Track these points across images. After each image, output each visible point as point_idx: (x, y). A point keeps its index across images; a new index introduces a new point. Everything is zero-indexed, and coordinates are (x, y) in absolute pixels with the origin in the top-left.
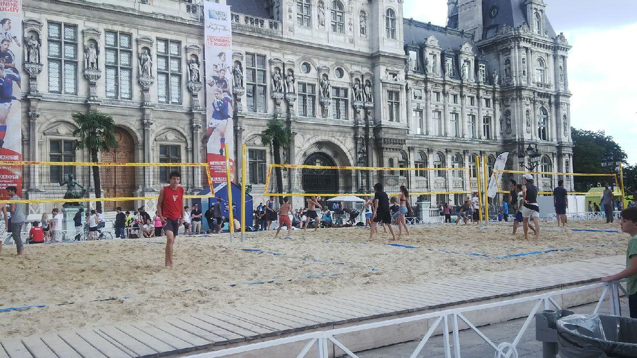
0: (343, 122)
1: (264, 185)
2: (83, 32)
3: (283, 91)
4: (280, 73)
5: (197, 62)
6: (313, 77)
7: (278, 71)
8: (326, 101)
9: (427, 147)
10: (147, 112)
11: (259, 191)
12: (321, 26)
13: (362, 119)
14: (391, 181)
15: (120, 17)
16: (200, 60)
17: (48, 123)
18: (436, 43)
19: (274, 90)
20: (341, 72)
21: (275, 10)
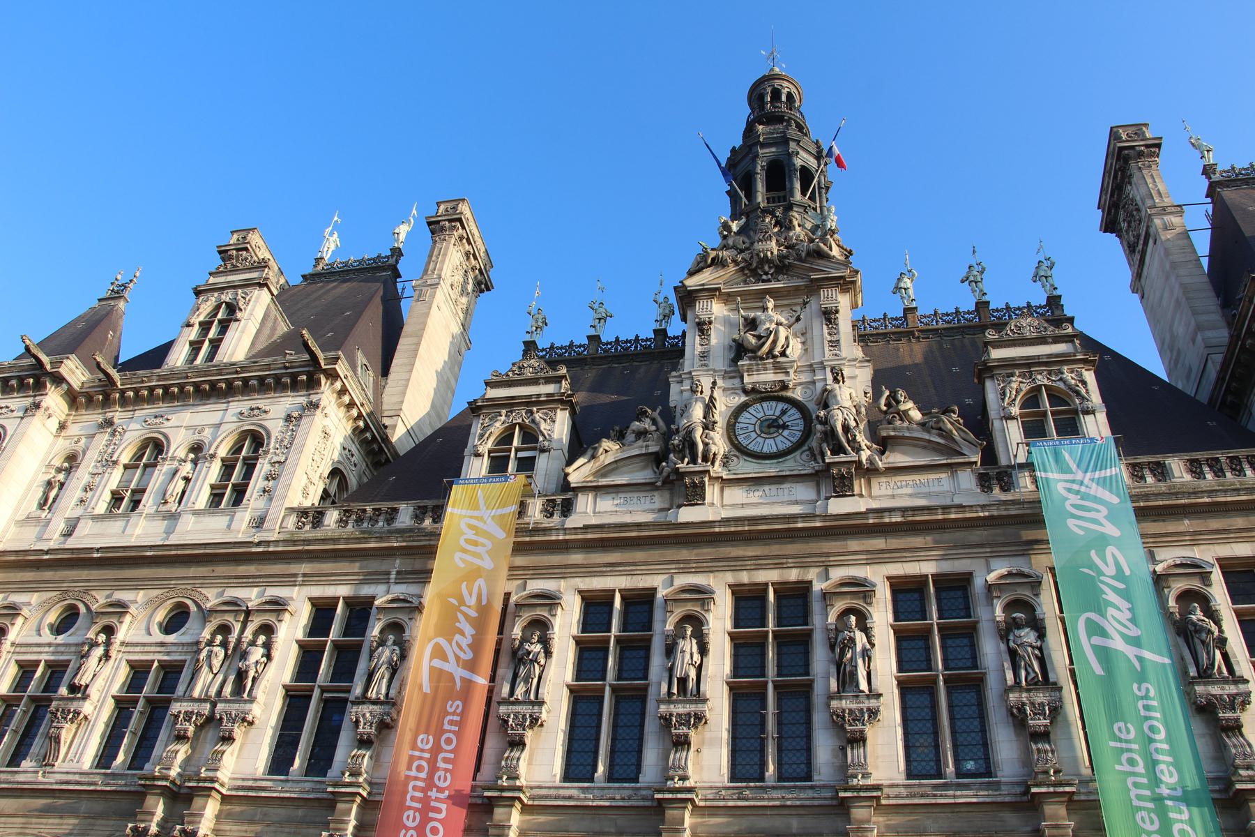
15: (775, 549)
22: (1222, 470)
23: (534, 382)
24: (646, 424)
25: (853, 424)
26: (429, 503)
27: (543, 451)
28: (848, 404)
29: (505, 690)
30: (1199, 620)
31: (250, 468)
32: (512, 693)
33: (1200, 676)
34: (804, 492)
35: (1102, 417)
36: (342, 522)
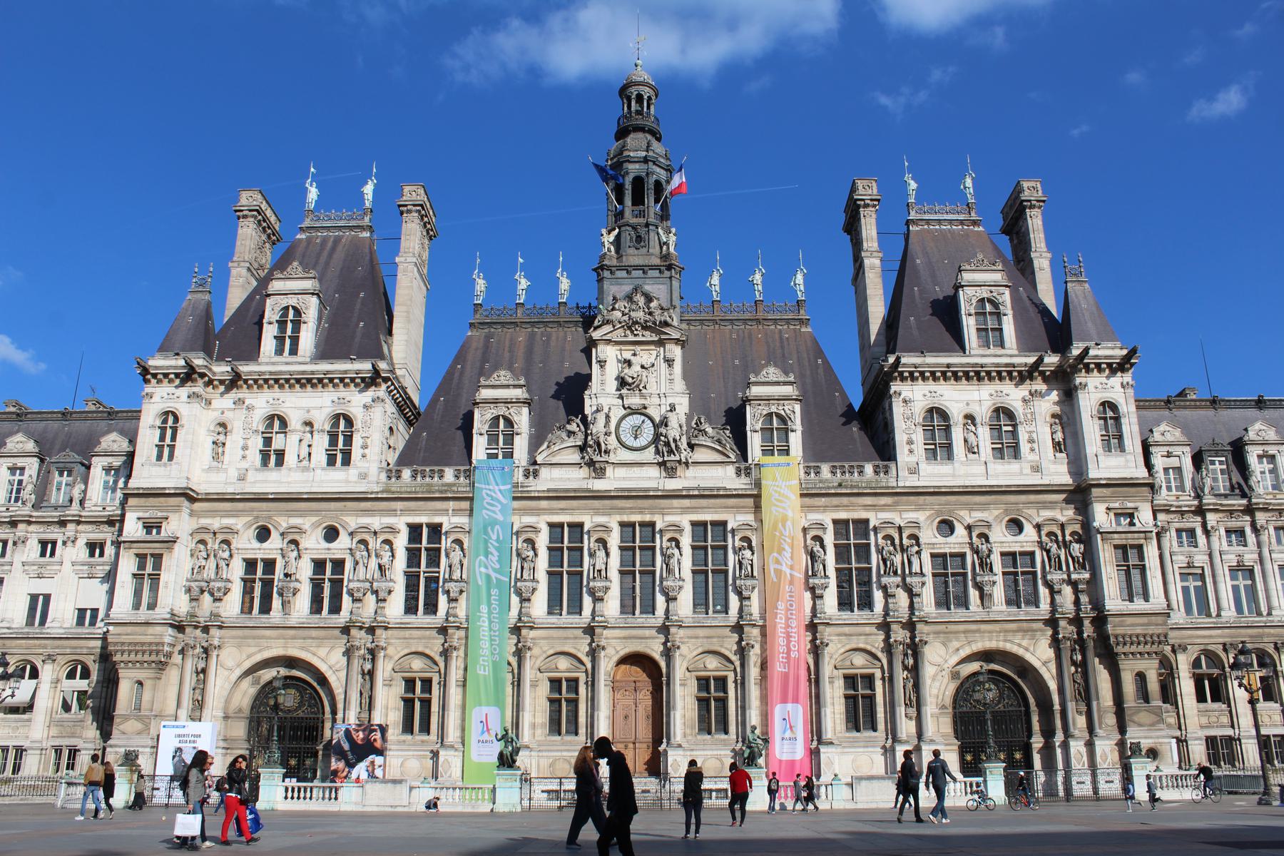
0: (1027, 613)
1: (873, 734)
2: (589, 532)
3: (899, 572)
4: (893, 544)
5: (750, 547)
6: (960, 540)
7: (889, 542)
8: (986, 578)
9: (1272, 639)
10: (673, 630)
11: (862, 744)
12: (971, 456)
13: (1069, 602)
14: (1144, 717)
15: (640, 503)
16: (754, 544)
17: (545, 656)
18: (1271, 435)
19: (882, 572)
20: (1016, 525)
21: (891, 443)
22: (844, 472)
23: (507, 386)
24: (573, 427)
25: (678, 438)
26: (462, 468)
27: (517, 434)
28: (676, 426)
29: (519, 576)
30: (818, 551)
31: (349, 440)
32: (522, 576)
33: (813, 575)
34: (654, 472)
35: (799, 433)
36: (414, 477)
